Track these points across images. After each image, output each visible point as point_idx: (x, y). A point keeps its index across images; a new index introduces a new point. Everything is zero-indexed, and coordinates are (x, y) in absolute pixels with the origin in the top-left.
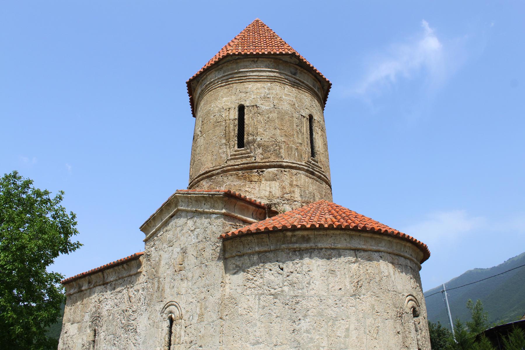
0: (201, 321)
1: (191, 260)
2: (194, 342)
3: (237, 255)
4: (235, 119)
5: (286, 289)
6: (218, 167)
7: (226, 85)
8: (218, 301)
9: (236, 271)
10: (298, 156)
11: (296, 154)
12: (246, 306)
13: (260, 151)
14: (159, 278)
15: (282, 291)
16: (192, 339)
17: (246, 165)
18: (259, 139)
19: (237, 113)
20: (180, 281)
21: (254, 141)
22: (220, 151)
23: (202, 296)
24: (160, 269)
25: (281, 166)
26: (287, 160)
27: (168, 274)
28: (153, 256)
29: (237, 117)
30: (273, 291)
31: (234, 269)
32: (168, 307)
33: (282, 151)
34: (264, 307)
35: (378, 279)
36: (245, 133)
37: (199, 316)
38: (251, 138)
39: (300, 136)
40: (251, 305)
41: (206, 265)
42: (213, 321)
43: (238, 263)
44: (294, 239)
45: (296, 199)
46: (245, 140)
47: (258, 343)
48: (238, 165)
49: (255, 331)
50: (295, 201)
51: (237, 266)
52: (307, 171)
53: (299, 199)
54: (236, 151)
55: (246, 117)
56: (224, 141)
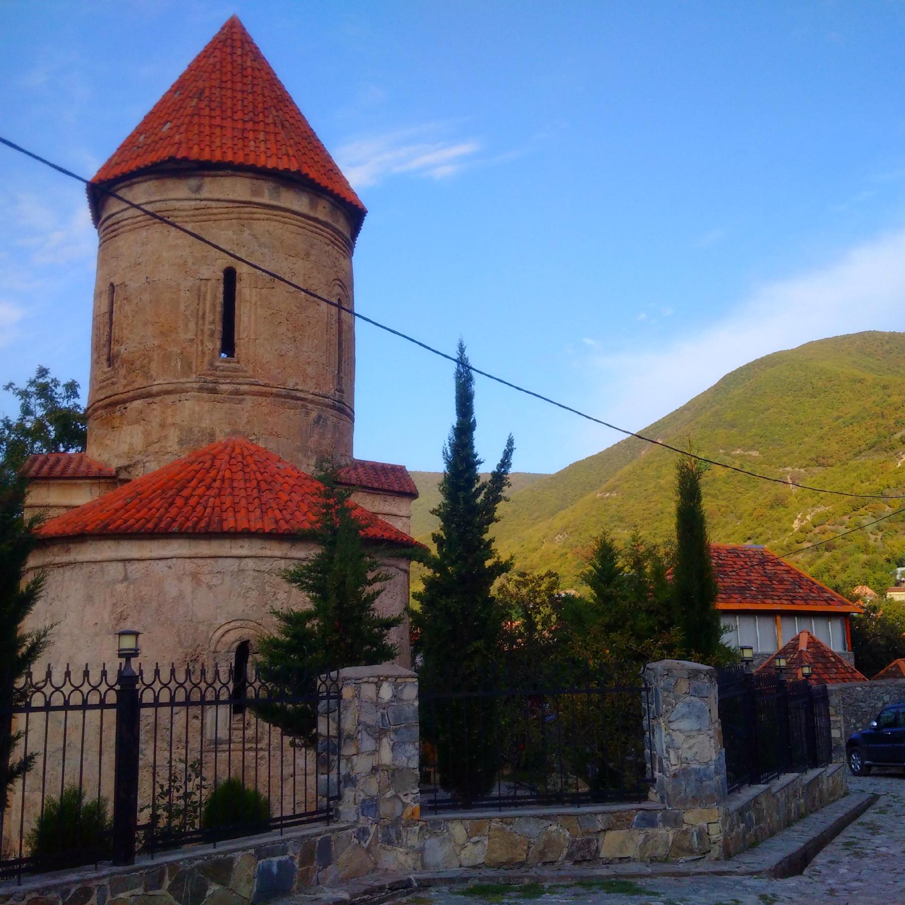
10: (182, 367)
11: (179, 364)
25: (150, 395)
26: (160, 382)
33: (154, 365)
35: (154, 605)
39: (192, 325)
45: (169, 450)
50: (168, 453)
52: (200, 389)
53: (176, 447)
54: (105, 373)
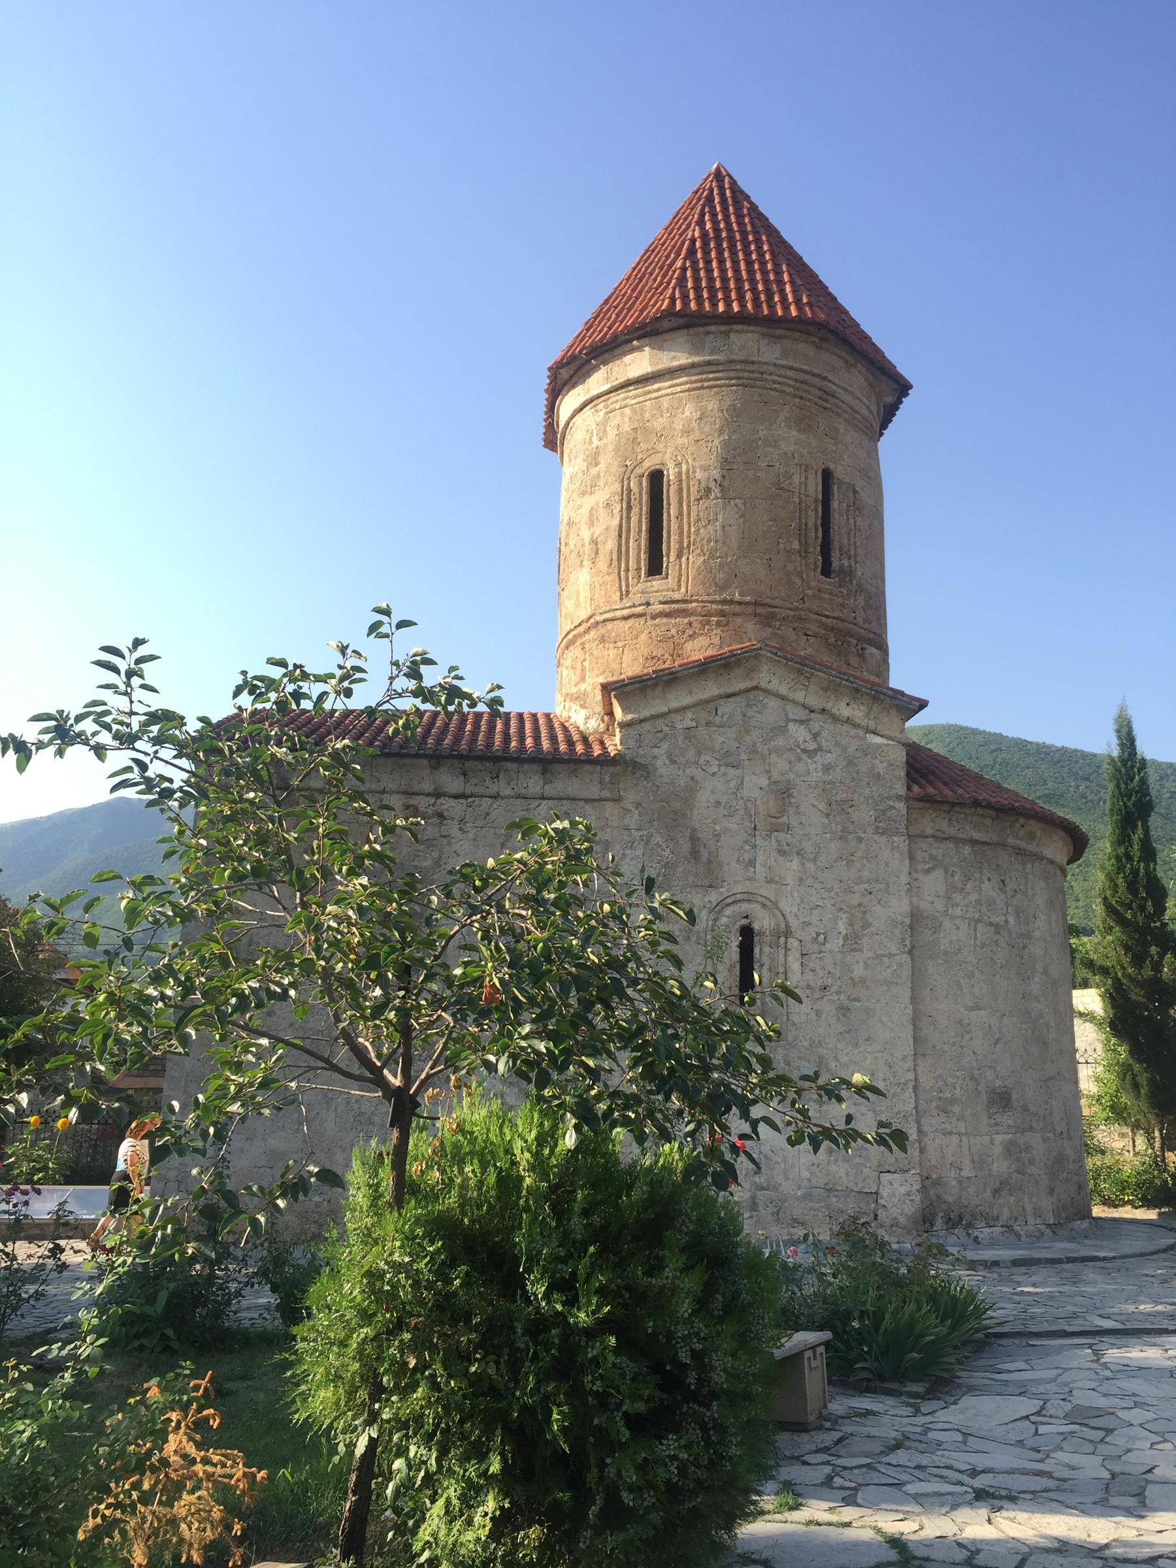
0: (852, 950)
1: (810, 814)
2: (835, 988)
3: (933, 836)
4: (816, 500)
5: (1011, 919)
6: (787, 605)
7: (795, 396)
8: (899, 918)
9: (927, 866)
12: (954, 939)
13: (861, 601)
14: (694, 830)
15: (1007, 922)
16: (829, 981)
17: (841, 625)
18: (859, 573)
19: (820, 488)
20: (775, 854)
21: (850, 573)
22: (790, 567)
23: (855, 899)
24: (695, 812)
27: (728, 829)
28: (662, 771)
29: (820, 497)
30: (994, 919)
31: (924, 862)
32: (735, 902)
34: (983, 946)
36: (836, 544)
37: (846, 938)
38: (846, 562)
40: (963, 938)
41: (860, 840)
42: (890, 956)
43: (934, 852)
44: (1022, 832)
46: (835, 564)
47: (977, 1007)
48: (827, 617)
49: (973, 986)
51: (932, 857)
55: (835, 504)
56: (796, 545)
